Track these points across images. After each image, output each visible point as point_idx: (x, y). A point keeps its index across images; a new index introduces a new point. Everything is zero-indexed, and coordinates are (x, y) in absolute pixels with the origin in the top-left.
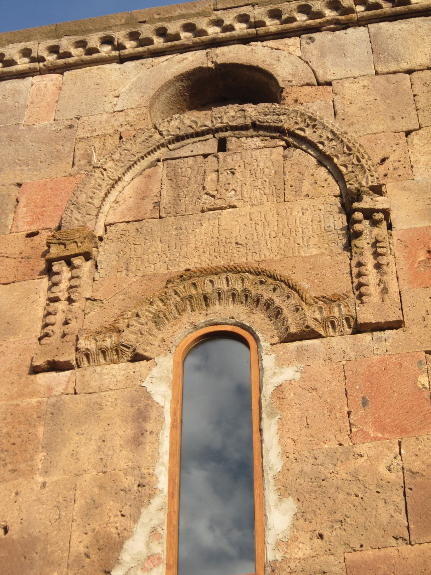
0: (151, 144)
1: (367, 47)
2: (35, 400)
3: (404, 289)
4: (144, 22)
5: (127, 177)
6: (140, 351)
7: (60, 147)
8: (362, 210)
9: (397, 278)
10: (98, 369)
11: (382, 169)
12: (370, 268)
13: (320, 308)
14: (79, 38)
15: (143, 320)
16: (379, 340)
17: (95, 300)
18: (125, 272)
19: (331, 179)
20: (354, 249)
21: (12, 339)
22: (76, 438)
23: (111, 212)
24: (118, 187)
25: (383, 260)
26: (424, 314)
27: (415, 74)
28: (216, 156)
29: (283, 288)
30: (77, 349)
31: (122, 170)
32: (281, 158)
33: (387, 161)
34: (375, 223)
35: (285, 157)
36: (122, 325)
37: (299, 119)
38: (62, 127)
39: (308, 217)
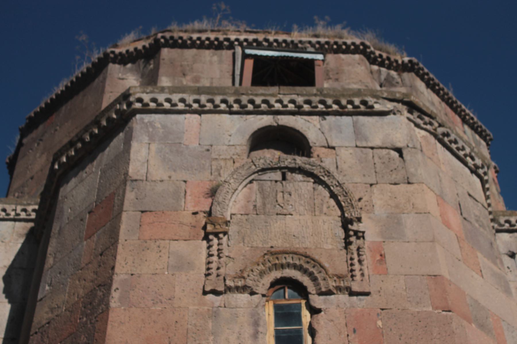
0: (251, 171)
1: (351, 129)
2: (206, 308)
3: (371, 274)
4: (243, 94)
5: (240, 188)
6: (254, 290)
7: (203, 162)
8: (353, 231)
9: (367, 267)
10: (235, 295)
11: (360, 204)
12: (356, 261)
13: (335, 281)
14: (210, 97)
15: (255, 273)
16: (360, 300)
17: (230, 257)
18: (242, 243)
19: (336, 207)
20: (349, 250)
21: (191, 272)
22: (228, 331)
23: (233, 207)
24: (236, 193)
25: (362, 258)
26: (379, 289)
27: (375, 150)
28: (282, 183)
29: (318, 267)
30: (225, 285)
31: (237, 184)
32: (312, 190)
33: (362, 201)
34: (358, 238)
35: (314, 189)
36: (245, 275)
37: (322, 170)
38: (204, 150)
39: (326, 227)
